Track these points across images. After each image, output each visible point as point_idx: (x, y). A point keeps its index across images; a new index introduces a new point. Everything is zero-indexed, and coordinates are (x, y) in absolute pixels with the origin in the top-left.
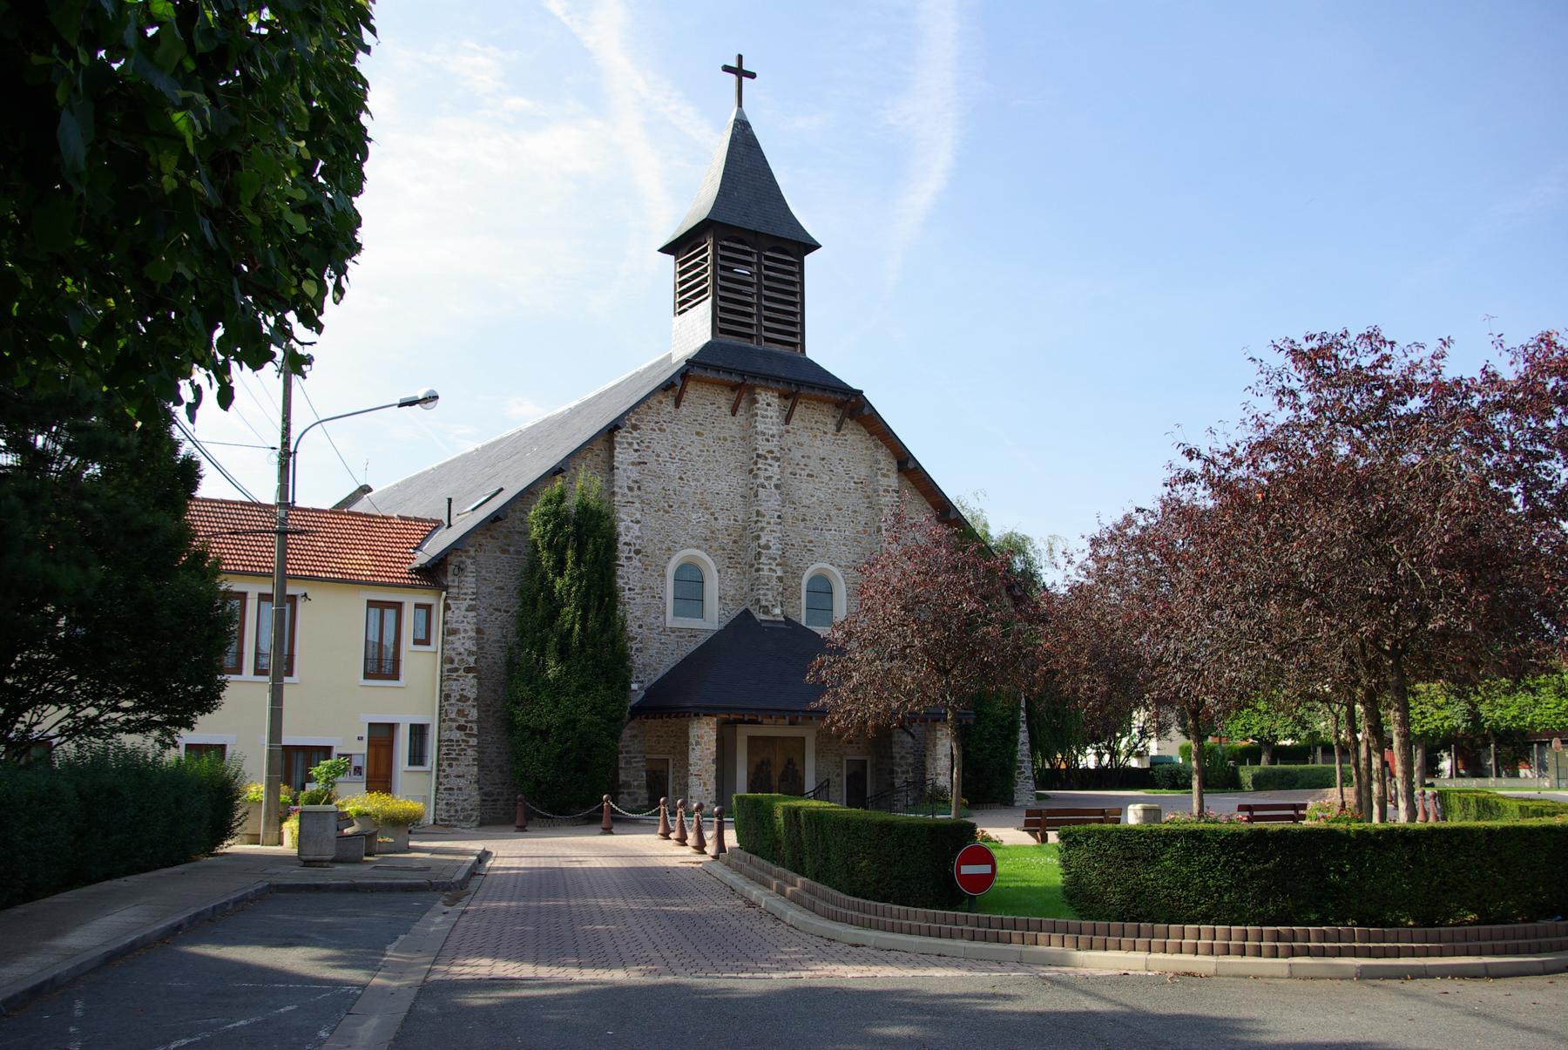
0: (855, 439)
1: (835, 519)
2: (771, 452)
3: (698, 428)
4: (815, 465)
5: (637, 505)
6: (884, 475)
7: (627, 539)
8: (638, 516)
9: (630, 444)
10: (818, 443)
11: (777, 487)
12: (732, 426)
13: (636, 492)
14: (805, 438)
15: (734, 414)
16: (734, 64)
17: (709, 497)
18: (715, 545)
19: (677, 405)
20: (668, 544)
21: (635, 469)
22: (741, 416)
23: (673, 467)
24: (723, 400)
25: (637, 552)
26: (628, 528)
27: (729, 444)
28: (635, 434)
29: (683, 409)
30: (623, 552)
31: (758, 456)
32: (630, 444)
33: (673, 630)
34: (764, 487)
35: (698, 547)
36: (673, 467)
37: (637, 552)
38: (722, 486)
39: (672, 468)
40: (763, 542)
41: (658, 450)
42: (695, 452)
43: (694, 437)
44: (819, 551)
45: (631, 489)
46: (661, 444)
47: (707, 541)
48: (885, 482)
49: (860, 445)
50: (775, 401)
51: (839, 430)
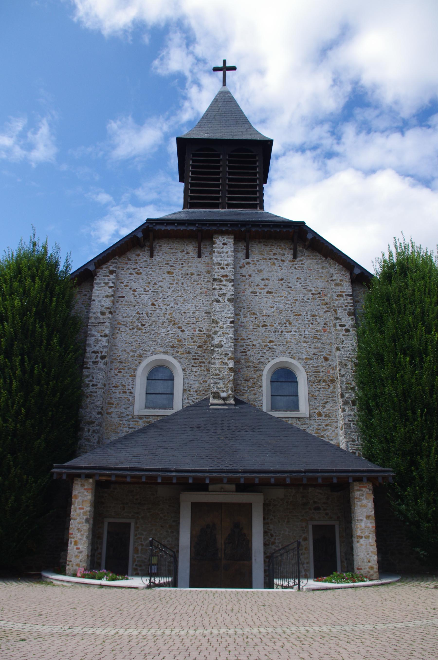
0: (310, 263)
1: (294, 323)
2: (226, 276)
3: (169, 269)
4: (273, 284)
5: (107, 324)
6: (337, 285)
7: (95, 349)
8: (107, 332)
9: (107, 284)
10: (277, 268)
11: (229, 300)
12: (197, 265)
13: (108, 315)
14: (264, 266)
15: (199, 256)
16: (221, 65)
17: (176, 316)
18: (181, 350)
19: (152, 256)
20: (139, 351)
21: (107, 299)
22: (205, 258)
23: (146, 298)
24: (191, 249)
25: (103, 358)
26: (97, 341)
27: (195, 277)
28: (112, 277)
29: (157, 258)
30: (90, 358)
31: (214, 280)
32: (107, 284)
33: (140, 417)
34: (218, 301)
35: (166, 353)
36: (146, 298)
37: (103, 358)
38: (190, 307)
39: (146, 299)
40: (216, 341)
41: (134, 286)
42: (166, 284)
43: (166, 276)
44: (279, 349)
45: (103, 313)
46: (138, 283)
47: (175, 348)
48: (339, 288)
49: (316, 267)
50: (230, 241)
51: (295, 257)
